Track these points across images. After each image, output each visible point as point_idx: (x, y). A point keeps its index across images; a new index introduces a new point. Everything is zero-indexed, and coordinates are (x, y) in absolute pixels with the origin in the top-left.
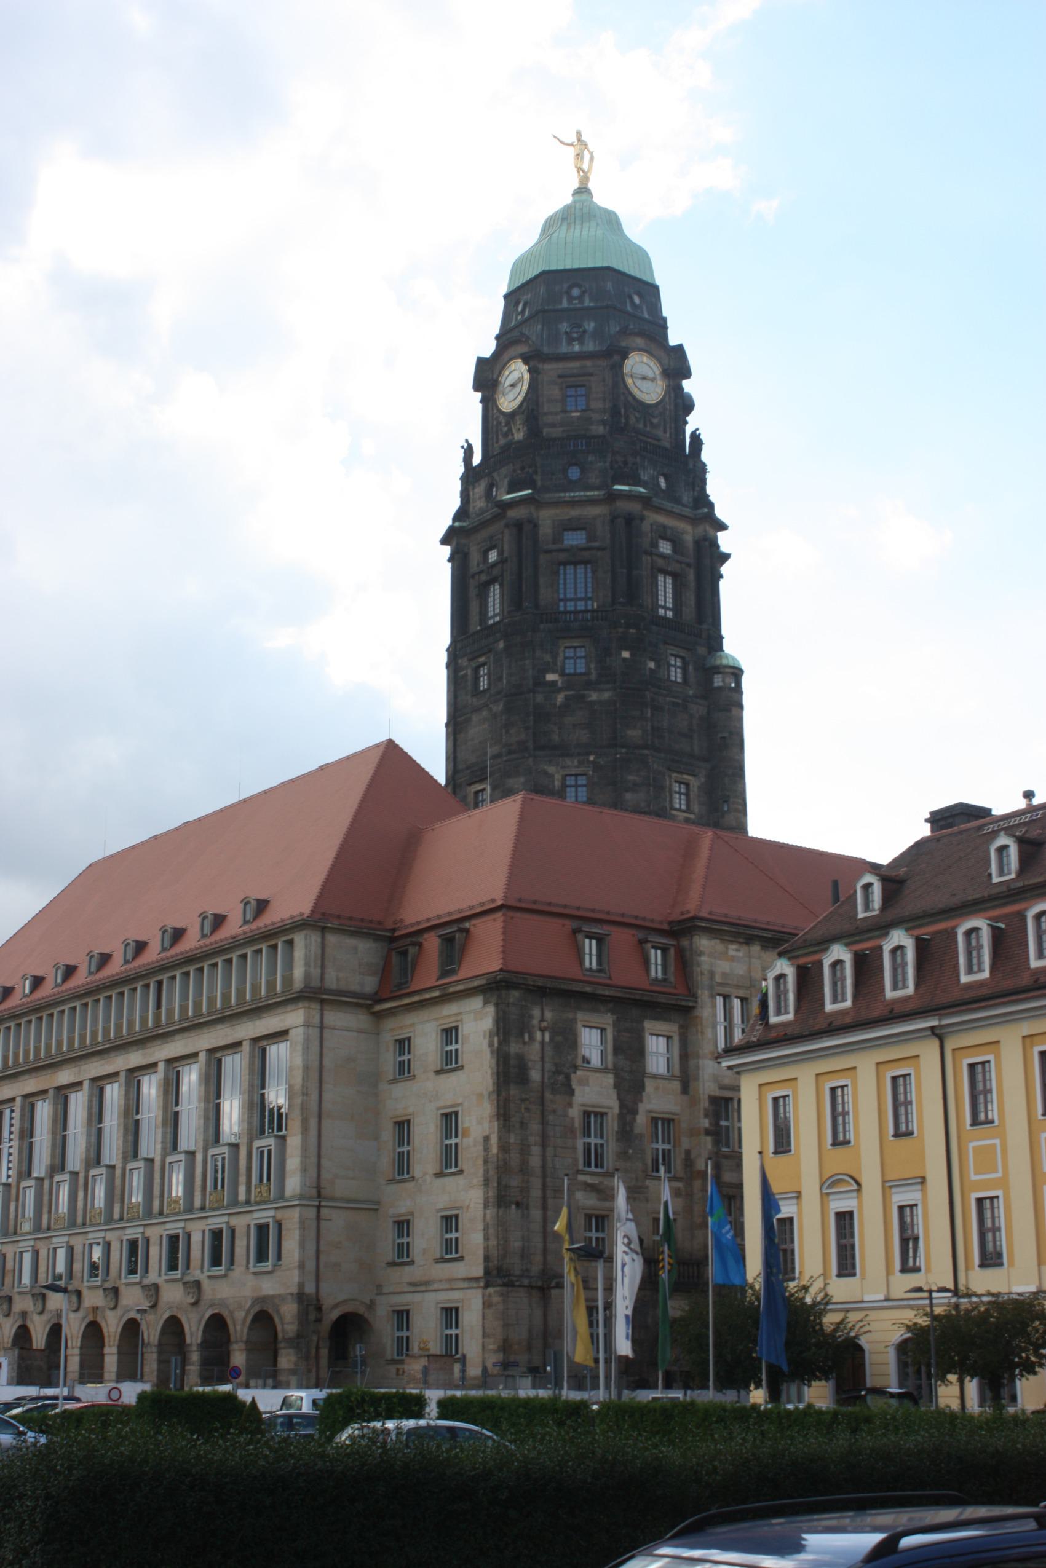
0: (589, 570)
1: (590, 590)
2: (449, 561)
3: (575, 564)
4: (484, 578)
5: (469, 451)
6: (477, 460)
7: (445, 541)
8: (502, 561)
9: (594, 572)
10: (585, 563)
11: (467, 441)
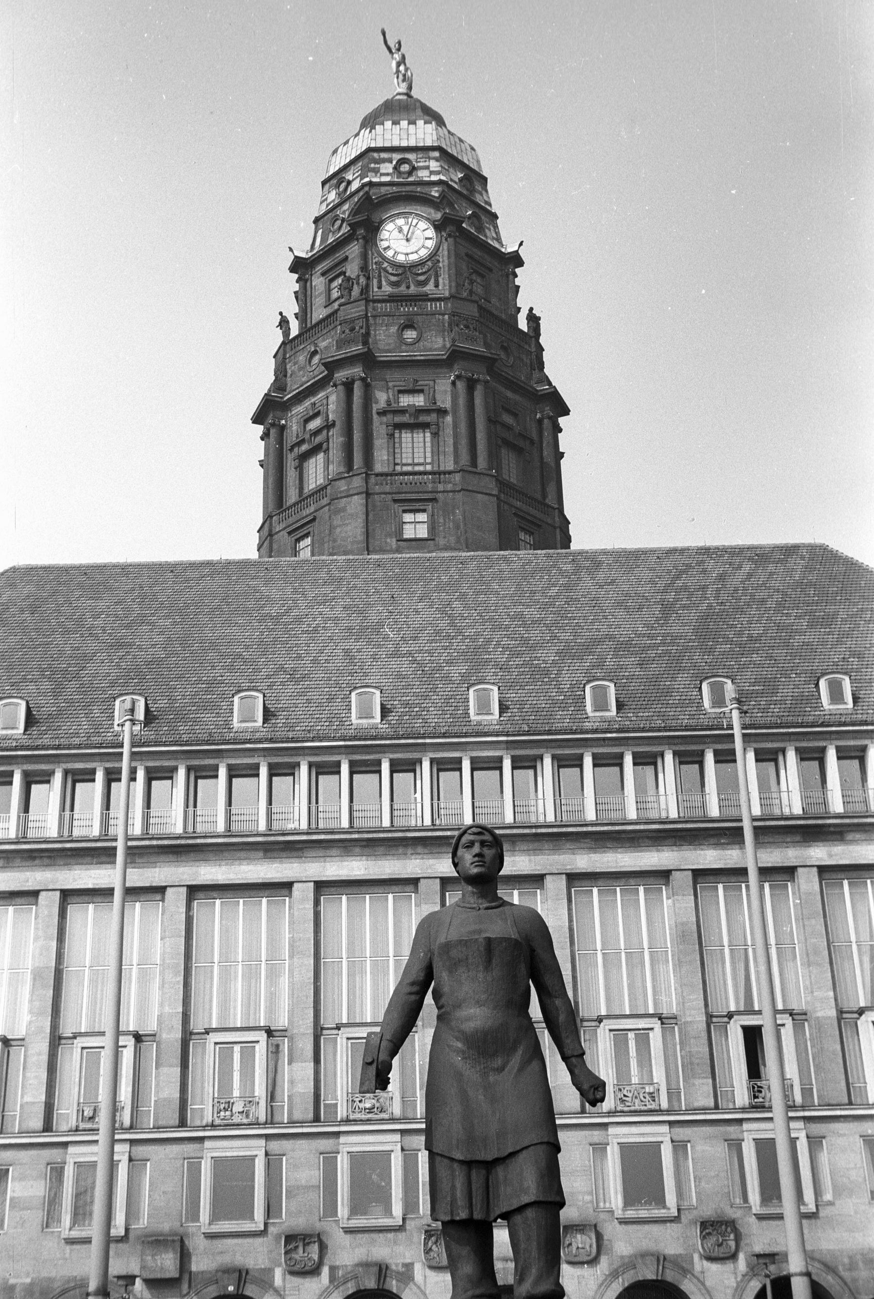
0: (428, 435)
1: (429, 455)
2: (262, 439)
3: (412, 427)
4: (304, 447)
5: (284, 323)
6: (295, 329)
7: (257, 419)
8: (329, 426)
9: (435, 435)
10: (424, 426)
11: (281, 314)
